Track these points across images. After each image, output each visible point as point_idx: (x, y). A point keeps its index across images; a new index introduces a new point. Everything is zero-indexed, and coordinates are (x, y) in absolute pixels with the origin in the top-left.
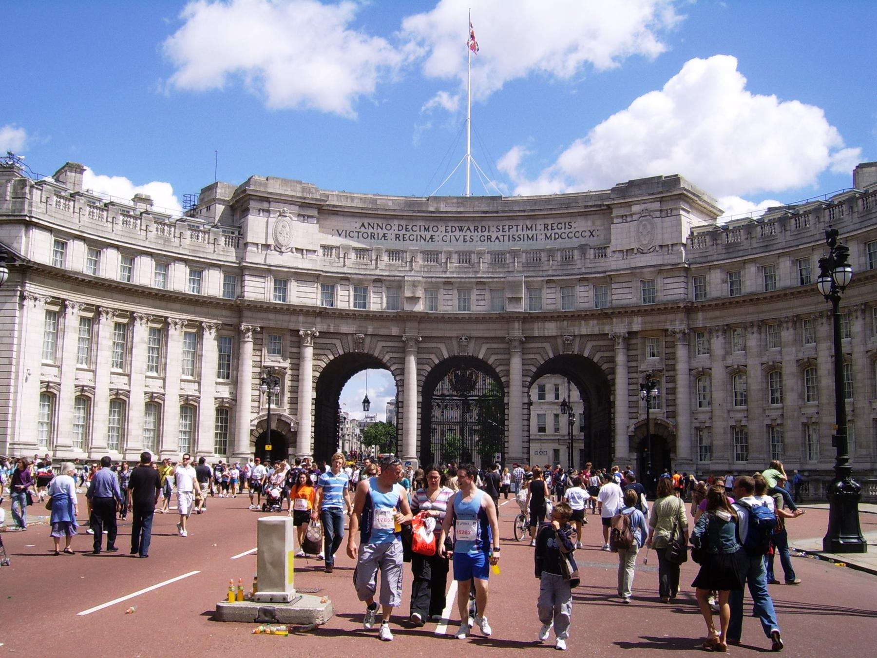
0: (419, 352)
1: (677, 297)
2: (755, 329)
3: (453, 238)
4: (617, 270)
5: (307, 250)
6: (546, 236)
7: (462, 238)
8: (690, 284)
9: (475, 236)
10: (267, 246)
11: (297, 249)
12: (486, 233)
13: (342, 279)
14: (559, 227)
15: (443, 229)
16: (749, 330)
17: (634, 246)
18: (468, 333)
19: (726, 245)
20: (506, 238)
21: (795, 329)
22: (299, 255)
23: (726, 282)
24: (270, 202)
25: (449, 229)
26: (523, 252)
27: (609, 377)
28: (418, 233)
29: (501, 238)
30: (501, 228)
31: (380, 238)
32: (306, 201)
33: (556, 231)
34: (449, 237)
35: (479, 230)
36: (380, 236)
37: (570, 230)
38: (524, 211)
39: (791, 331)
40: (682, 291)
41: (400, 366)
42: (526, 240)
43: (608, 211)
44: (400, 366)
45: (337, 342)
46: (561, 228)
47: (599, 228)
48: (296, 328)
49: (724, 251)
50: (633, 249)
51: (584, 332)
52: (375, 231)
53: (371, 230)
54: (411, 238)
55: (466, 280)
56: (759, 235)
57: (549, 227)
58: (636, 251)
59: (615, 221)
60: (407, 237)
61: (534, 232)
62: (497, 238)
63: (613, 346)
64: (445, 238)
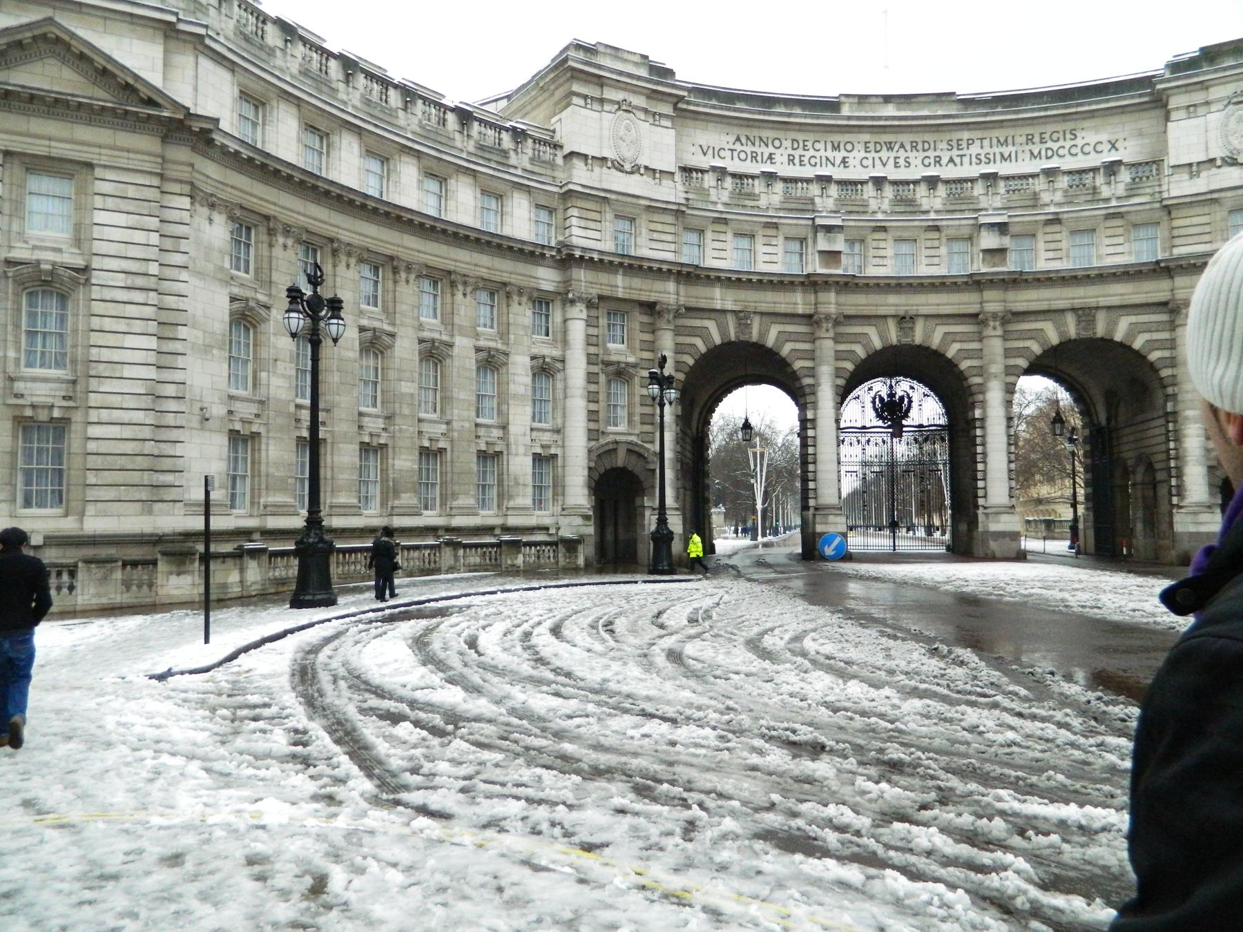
5: (661, 172)
6: (1032, 153)
7: (891, 161)
10: (604, 159)
11: (646, 168)
12: (931, 154)
13: (717, 221)
15: (861, 147)
17: (1217, 152)
18: (913, 310)
22: (650, 180)
24: (602, 86)
25: (871, 146)
27: (1165, 373)
28: (822, 153)
29: (957, 160)
30: (954, 143)
32: (660, 88)
33: (1050, 144)
35: (920, 147)
36: (765, 158)
41: (808, 364)
44: (808, 364)
45: (711, 325)
46: (1058, 140)
48: (652, 299)
50: (1212, 161)
51: (1115, 301)
54: (813, 161)
55: (911, 224)
57: (1037, 139)
58: (1219, 163)
59: (1174, 116)
60: (806, 159)
62: (951, 160)
63: (1172, 322)
64: (865, 162)
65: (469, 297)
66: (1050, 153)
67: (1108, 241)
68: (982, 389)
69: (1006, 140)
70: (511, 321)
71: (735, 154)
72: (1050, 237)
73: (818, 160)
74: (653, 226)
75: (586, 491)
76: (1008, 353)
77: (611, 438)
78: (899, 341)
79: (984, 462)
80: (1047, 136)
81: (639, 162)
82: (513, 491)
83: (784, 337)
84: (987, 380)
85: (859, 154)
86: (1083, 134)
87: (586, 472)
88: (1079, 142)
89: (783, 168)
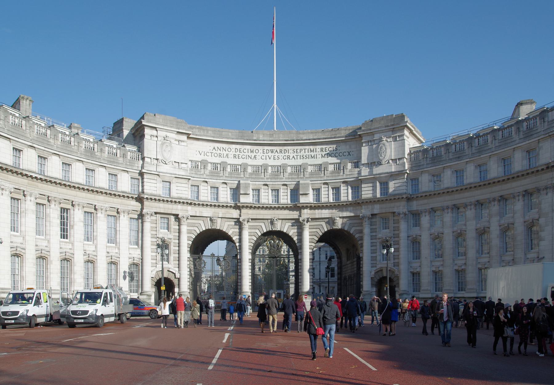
1: (402, 192)
2: (450, 210)
3: (267, 157)
4: (365, 176)
6: (322, 156)
7: (273, 157)
8: (409, 183)
9: (280, 156)
12: (287, 154)
15: (261, 151)
16: (446, 211)
19: (432, 158)
20: (299, 157)
21: (476, 209)
23: (431, 181)
25: (265, 151)
26: (309, 165)
29: (295, 157)
30: (295, 151)
35: (283, 152)
36: (225, 156)
37: (337, 152)
38: (309, 140)
39: (473, 210)
40: (405, 187)
43: (359, 139)
47: (353, 150)
49: (431, 162)
50: (375, 162)
52: (221, 152)
54: (243, 157)
56: (454, 151)
57: (324, 150)
58: (376, 163)
59: (364, 145)
61: (315, 153)
62: (293, 157)
69: (313, 150)
73: (245, 157)
85: (260, 154)
89: (231, 161)
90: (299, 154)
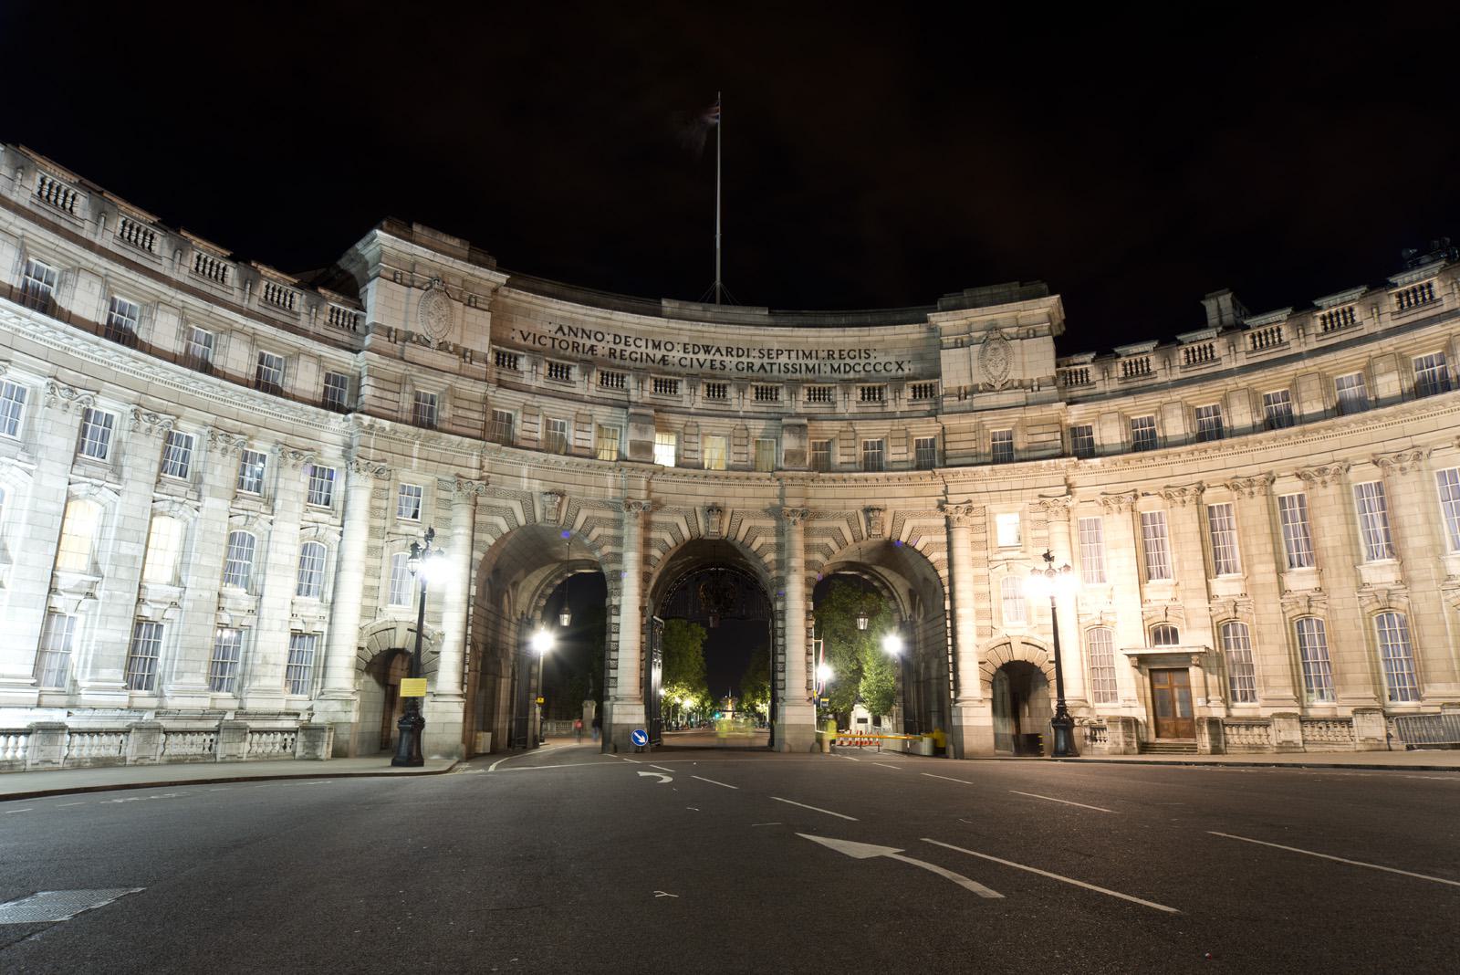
0: (647, 526)
3: (695, 361)
6: (832, 367)
12: (744, 359)
14: (852, 354)
15: (680, 347)
17: (980, 379)
27: (944, 573)
29: (768, 368)
30: (765, 352)
31: (586, 349)
33: (848, 361)
34: (689, 360)
35: (734, 353)
36: (586, 349)
42: (803, 372)
52: (578, 340)
53: (571, 338)
54: (634, 356)
57: (836, 355)
60: (627, 354)
61: (814, 361)
62: (762, 366)
65: (228, 457)
66: (848, 369)
67: (892, 450)
68: (782, 582)
70: (281, 485)
71: (557, 342)
72: (844, 443)
73: (639, 356)
74: (458, 403)
75: (351, 673)
76: (808, 548)
77: (391, 614)
78: (707, 532)
79: (784, 654)
80: (845, 353)
81: (447, 339)
82: (258, 670)
83: (590, 523)
84: (789, 573)
86: (875, 354)
87: (354, 652)
88: (873, 361)
90: (779, 361)
